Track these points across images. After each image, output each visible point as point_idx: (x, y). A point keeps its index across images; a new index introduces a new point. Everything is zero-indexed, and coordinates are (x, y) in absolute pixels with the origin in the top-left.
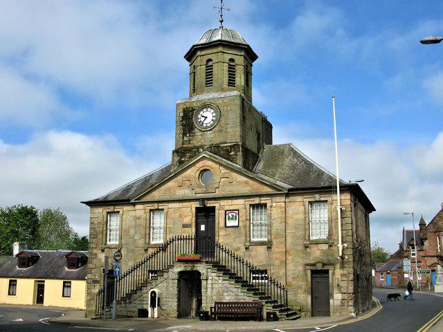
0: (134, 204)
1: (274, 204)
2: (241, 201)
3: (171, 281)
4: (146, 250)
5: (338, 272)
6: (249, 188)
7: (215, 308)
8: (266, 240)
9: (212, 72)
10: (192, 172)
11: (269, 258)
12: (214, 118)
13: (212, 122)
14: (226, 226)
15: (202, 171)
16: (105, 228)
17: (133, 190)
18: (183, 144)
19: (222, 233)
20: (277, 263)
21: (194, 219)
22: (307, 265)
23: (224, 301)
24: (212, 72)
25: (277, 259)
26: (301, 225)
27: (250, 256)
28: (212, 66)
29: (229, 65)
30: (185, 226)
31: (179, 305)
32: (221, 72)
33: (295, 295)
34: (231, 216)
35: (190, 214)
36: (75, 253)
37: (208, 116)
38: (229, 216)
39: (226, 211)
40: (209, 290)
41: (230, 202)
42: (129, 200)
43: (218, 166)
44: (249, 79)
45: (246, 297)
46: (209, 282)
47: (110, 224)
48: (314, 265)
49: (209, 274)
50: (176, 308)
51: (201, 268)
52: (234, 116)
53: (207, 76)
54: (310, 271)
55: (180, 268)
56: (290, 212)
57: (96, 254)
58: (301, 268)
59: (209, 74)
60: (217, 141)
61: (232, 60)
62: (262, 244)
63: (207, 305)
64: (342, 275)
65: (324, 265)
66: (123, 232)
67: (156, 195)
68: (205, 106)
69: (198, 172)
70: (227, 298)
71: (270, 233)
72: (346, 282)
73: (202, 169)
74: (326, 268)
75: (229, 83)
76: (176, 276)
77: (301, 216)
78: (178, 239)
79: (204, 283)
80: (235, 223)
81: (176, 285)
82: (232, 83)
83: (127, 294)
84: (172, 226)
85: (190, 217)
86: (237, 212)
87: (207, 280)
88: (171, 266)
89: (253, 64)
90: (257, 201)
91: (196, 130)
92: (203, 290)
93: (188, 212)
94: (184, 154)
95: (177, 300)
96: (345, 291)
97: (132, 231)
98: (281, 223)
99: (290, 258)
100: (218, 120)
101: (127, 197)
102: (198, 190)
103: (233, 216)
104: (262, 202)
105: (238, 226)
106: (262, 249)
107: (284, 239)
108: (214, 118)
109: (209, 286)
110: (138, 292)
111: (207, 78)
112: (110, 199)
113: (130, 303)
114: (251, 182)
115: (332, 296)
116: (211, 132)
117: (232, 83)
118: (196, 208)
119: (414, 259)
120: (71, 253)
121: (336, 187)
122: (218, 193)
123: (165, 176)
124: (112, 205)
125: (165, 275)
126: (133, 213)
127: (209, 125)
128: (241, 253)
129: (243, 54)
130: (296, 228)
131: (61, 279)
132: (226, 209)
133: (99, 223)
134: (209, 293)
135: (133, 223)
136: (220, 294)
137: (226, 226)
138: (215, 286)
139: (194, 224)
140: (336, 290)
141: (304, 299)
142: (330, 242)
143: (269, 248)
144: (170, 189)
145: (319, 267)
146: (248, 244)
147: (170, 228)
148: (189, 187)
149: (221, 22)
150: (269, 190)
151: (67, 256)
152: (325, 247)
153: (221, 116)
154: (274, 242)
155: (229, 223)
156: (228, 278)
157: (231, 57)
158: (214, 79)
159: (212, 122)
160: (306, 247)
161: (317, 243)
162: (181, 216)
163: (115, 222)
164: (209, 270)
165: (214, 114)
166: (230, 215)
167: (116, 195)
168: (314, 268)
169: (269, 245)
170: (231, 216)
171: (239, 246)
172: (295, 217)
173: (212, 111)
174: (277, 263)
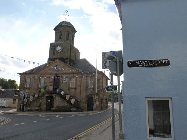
8: (74, 87)
14: (63, 83)
19: (62, 85)
20: (78, 94)
21: (53, 80)
22: (86, 95)
27: (69, 92)
30: (50, 82)
31: (46, 107)
32: (64, 35)
37: (59, 49)
45: (67, 105)
46: (56, 99)
50: (45, 108)
51: (54, 96)
58: (85, 96)
60: (62, 56)
61: (68, 31)
66: (31, 84)
67: (42, 72)
70: (61, 105)
71: (76, 85)
76: (46, 98)
77: (85, 80)
82: (68, 38)
87: (55, 99)
88: (44, 95)
92: (54, 102)
94: (51, 60)
97: (34, 84)
99: (81, 93)
100: (62, 51)
107: (80, 87)
109: (56, 101)
110: (34, 102)
117: (68, 38)
123: (45, 66)
134: (56, 103)
137: (63, 83)
138: (58, 101)
139: (53, 82)
141: (86, 106)
142: (94, 89)
145: (90, 96)
149: (66, 19)
153: (63, 49)
155: (64, 82)
161: (90, 88)
163: (28, 80)
169: (75, 89)
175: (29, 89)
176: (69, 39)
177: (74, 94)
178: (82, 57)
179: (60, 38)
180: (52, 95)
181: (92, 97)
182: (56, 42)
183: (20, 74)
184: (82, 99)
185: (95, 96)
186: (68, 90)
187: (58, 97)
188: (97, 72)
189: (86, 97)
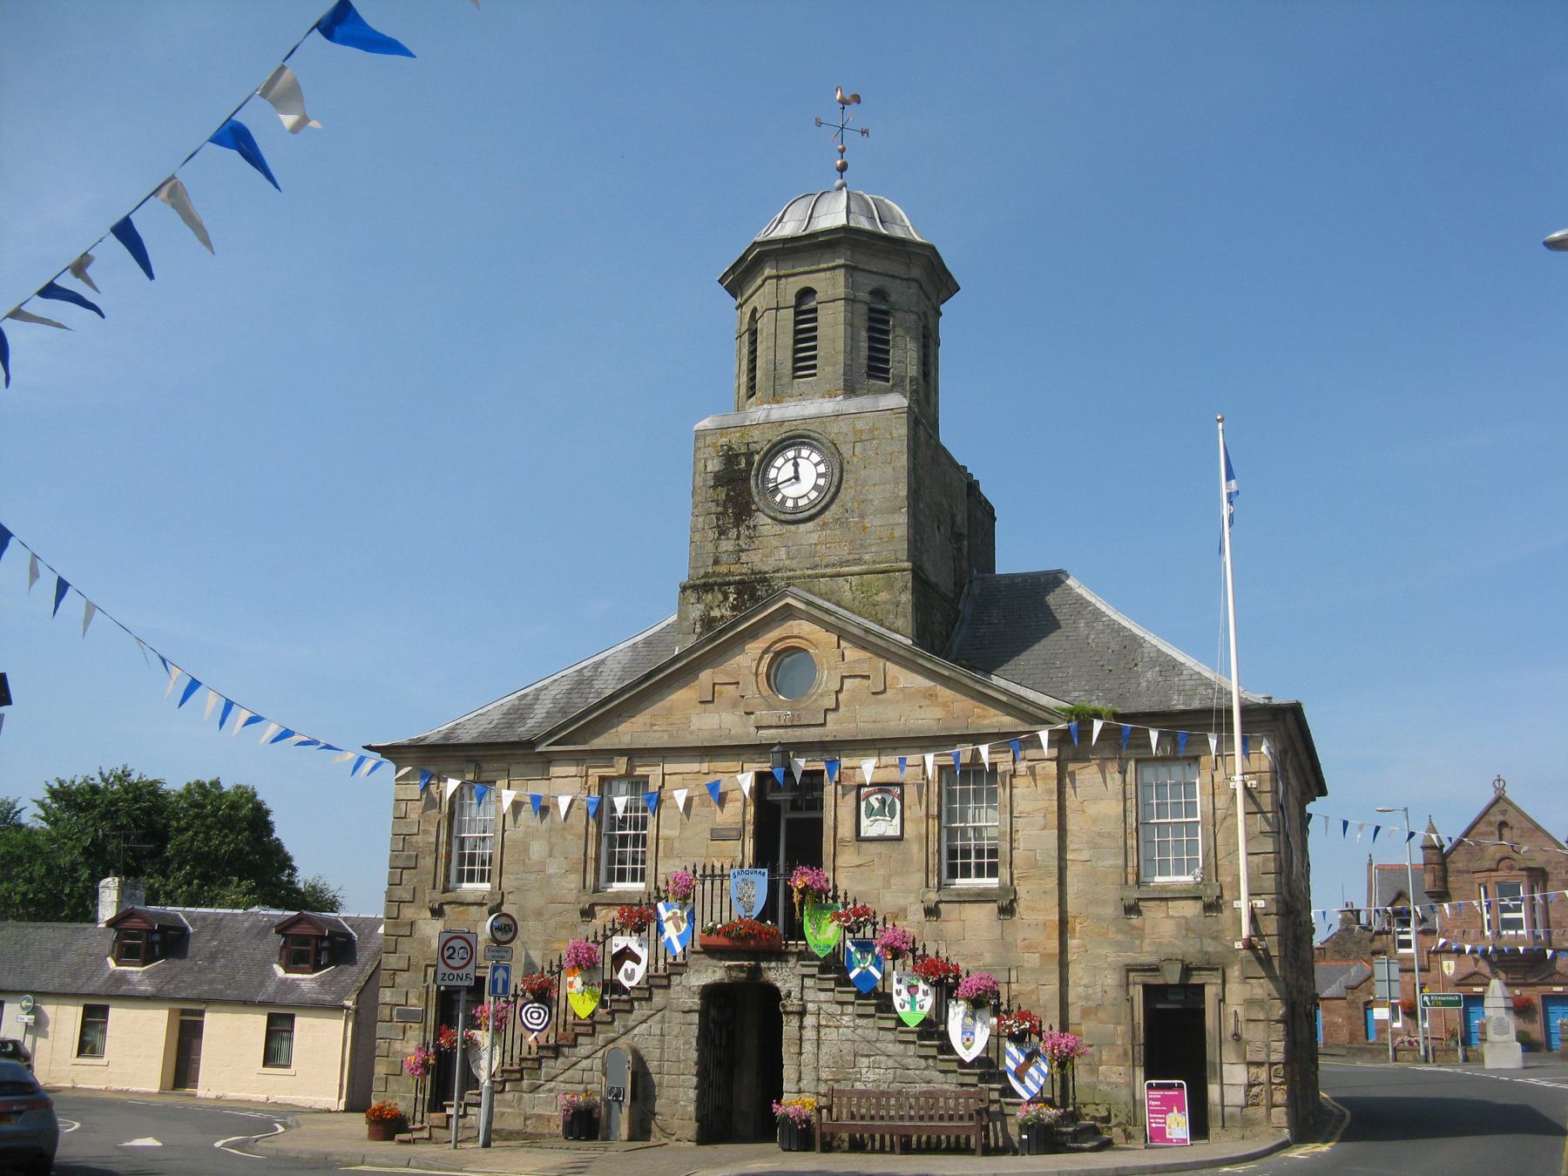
1: (1022, 767)
3: (679, 1017)
4: (588, 913)
5: (1237, 993)
6: (938, 713)
7: (830, 1110)
9: (815, 329)
10: (749, 659)
11: (1003, 944)
12: (821, 482)
13: (814, 495)
15: (778, 654)
16: (443, 837)
17: (540, 712)
18: (716, 562)
19: (847, 858)
21: (751, 810)
22: (1130, 969)
23: (859, 1086)
24: (815, 329)
28: (815, 310)
29: (871, 310)
30: (717, 835)
33: (1093, 1069)
36: (310, 921)
38: (869, 803)
40: (808, 1047)
42: (530, 744)
44: (932, 359)
46: (809, 1020)
47: (460, 822)
48: (1154, 969)
50: (692, 1108)
51: (783, 977)
52: (884, 483)
53: (796, 342)
54: (1140, 988)
55: (712, 973)
57: (412, 924)
58: (1111, 979)
59: (805, 335)
62: (981, 897)
63: (795, 1100)
64: (1250, 1003)
65: (1187, 970)
68: (793, 439)
69: (768, 658)
70: (870, 1076)
72: (1261, 1025)
73: (779, 646)
75: (870, 368)
76: (695, 1002)
78: (704, 876)
79: (789, 1027)
80: (890, 828)
81: (695, 1030)
83: (522, 1060)
84: (675, 833)
86: (898, 790)
87: (802, 1013)
89: (943, 308)
91: (761, 519)
92: (788, 1051)
95: (695, 1080)
96: (1261, 1057)
100: (831, 493)
101: (523, 731)
102: (765, 716)
103: (883, 802)
105: (900, 839)
106: (983, 915)
108: (821, 482)
109: (809, 1034)
111: (796, 351)
112: (466, 737)
113: (535, 1089)
114: (944, 692)
116: (810, 525)
119: (1410, 958)
120: (293, 922)
121: (1229, 712)
122: (835, 728)
124: (469, 760)
125: (659, 997)
127: (801, 502)
128: (913, 923)
129: (916, 272)
130: (1094, 845)
131: (262, 1004)
136: (846, 1067)
138: (829, 1034)
139: (750, 828)
140: (1229, 1054)
143: (1007, 910)
145: (1172, 976)
146: (933, 896)
147: (667, 839)
148: (734, 705)
150: (1006, 722)
151: (283, 928)
152: (1191, 909)
154: (1022, 891)
155: (870, 828)
156: (872, 1010)
157: (876, 282)
158: (820, 352)
159: (814, 495)
160: (1132, 909)
161: (1165, 897)
164: (809, 982)
165: (822, 468)
166: (873, 800)
167: (484, 725)
170: (876, 805)
171: (901, 902)
172: (1092, 809)
173: (815, 458)
174: (1032, 960)
176: (894, 368)
177: (988, 958)
178: (1013, 556)
179: (804, 362)
182: (759, 412)
183: (391, 752)
184: (1086, 1013)
185: (1234, 973)
186: (916, 914)
187: (823, 996)
188: (1246, 710)
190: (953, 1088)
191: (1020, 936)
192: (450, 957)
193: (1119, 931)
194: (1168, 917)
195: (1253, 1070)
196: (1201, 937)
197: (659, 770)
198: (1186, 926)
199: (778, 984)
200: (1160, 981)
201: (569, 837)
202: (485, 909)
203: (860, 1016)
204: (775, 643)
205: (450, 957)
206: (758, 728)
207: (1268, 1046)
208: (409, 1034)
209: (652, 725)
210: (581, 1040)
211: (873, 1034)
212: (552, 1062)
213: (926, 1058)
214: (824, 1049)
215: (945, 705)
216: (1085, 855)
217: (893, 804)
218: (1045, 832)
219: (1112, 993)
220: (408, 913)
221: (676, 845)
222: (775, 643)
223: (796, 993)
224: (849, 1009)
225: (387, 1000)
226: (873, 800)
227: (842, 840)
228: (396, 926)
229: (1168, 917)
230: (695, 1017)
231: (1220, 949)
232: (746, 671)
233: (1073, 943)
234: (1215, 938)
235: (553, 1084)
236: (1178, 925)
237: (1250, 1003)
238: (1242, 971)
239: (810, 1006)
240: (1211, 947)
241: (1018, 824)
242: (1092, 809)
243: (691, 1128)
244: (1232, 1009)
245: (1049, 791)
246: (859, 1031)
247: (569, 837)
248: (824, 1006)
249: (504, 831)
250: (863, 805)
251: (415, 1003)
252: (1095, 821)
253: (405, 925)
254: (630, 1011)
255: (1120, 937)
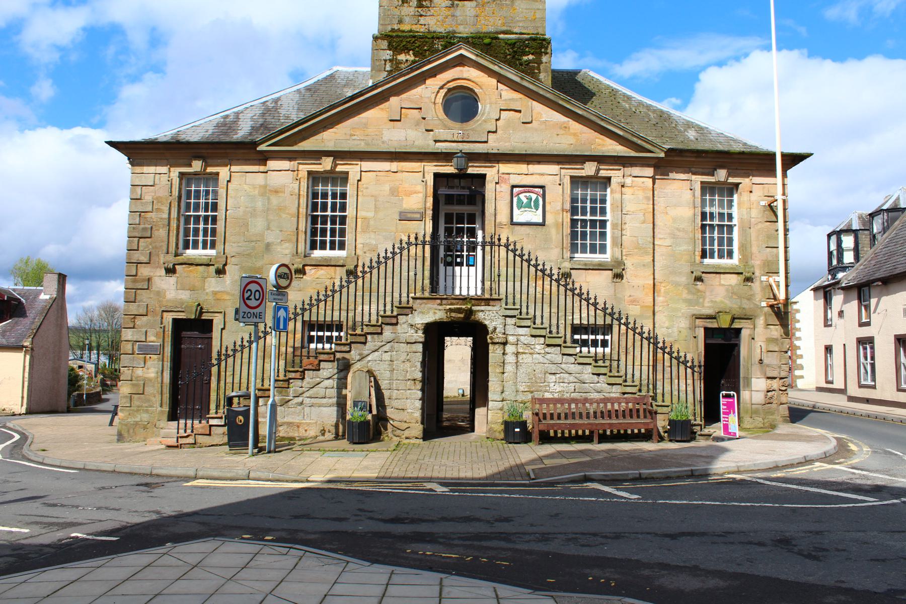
0: (263, 158)
1: (628, 181)
2: (554, 168)
6: (572, 140)
10: (429, 93)
14: (513, 223)
15: (449, 90)
21: (430, 200)
23: (548, 395)
25: (634, 302)
26: (684, 230)
30: (405, 217)
34: (525, 201)
35: (420, 188)
38: (519, 199)
39: (513, 187)
40: (509, 368)
41: (523, 168)
43: (494, 81)
46: (510, 349)
49: (510, 330)
50: (418, 415)
54: (702, 330)
56: (660, 203)
57: (149, 280)
58: (684, 324)
65: (733, 319)
67: (329, 139)
69: (443, 92)
70: (555, 388)
74: (736, 325)
76: (420, 336)
81: (419, 357)
84: (370, 214)
85: (421, 195)
86: (540, 191)
88: (406, 310)
90: (589, 169)
93: (415, 186)
95: (419, 394)
98: (644, 222)
104: (603, 173)
105: (543, 224)
109: (510, 358)
115: (748, 384)
118: (437, 176)
122: (494, 145)
125: (388, 332)
126: (260, 179)
130: (673, 236)
132: (515, 180)
133: (159, 200)
135: (259, 204)
138: (525, 359)
139: (430, 213)
143: (619, 276)
144: (366, 125)
147: (364, 218)
148: (417, 124)
152: (733, 280)
154: (628, 263)
155: (520, 216)
162: (394, 192)
168: (713, 325)
170: (525, 201)
172: (673, 212)
175: (220, 272)
180: (470, 312)
181: (739, 331)
185: (760, 321)
189: (693, 328)
190: (618, 395)
191: (628, 293)
192: (248, 299)
193: (690, 292)
194: (721, 285)
195: (769, 381)
196: (740, 297)
197: (357, 168)
198: (732, 292)
199: (487, 322)
200: (715, 325)
201: (284, 216)
202: (212, 269)
203: (548, 345)
204: (449, 82)
205: (248, 299)
206: (436, 141)
207: (780, 367)
208: (149, 363)
209: (352, 135)
210: (323, 365)
211: (559, 358)
212: (299, 383)
213: (598, 375)
214: (522, 370)
215: (575, 135)
216: (668, 242)
217: (537, 201)
218: (644, 226)
219: (685, 333)
220: (145, 271)
221: (372, 223)
222: (449, 82)
223: (500, 329)
224: (542, 340)
225: (130, 338)
226: (522, 196)
227: (500, 224)
228: (135, 281)
229: (721, 285)
230: (420, 347)
231: (752, 306)
232: (427, 100)
233: (659, 299)
234: (749, 299)
235: (300, 399)
236: (727, 290)
237: (770, 340)
238: (766, 320)
239: (511, 339)
240: (746, 305)
241: (627, 218)
242: (673, 212)
243: (417, 429)
244: (760, 343)
245: (647, 198)
246: (548, 356)
247: (284, 216)
248: (522, 338)
249: (227, 210)
250: (515, 200)
251: (153, 339)
252: (674, 220)
253: (143, 280)
254: (365, 343)
255: (690, 297)
